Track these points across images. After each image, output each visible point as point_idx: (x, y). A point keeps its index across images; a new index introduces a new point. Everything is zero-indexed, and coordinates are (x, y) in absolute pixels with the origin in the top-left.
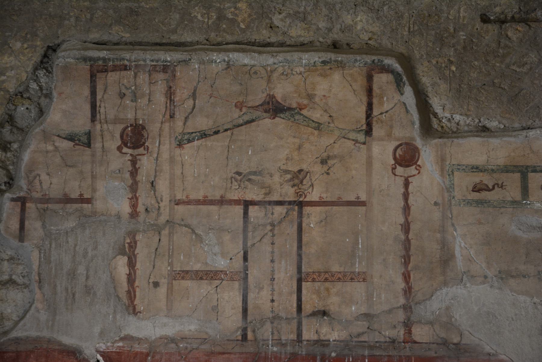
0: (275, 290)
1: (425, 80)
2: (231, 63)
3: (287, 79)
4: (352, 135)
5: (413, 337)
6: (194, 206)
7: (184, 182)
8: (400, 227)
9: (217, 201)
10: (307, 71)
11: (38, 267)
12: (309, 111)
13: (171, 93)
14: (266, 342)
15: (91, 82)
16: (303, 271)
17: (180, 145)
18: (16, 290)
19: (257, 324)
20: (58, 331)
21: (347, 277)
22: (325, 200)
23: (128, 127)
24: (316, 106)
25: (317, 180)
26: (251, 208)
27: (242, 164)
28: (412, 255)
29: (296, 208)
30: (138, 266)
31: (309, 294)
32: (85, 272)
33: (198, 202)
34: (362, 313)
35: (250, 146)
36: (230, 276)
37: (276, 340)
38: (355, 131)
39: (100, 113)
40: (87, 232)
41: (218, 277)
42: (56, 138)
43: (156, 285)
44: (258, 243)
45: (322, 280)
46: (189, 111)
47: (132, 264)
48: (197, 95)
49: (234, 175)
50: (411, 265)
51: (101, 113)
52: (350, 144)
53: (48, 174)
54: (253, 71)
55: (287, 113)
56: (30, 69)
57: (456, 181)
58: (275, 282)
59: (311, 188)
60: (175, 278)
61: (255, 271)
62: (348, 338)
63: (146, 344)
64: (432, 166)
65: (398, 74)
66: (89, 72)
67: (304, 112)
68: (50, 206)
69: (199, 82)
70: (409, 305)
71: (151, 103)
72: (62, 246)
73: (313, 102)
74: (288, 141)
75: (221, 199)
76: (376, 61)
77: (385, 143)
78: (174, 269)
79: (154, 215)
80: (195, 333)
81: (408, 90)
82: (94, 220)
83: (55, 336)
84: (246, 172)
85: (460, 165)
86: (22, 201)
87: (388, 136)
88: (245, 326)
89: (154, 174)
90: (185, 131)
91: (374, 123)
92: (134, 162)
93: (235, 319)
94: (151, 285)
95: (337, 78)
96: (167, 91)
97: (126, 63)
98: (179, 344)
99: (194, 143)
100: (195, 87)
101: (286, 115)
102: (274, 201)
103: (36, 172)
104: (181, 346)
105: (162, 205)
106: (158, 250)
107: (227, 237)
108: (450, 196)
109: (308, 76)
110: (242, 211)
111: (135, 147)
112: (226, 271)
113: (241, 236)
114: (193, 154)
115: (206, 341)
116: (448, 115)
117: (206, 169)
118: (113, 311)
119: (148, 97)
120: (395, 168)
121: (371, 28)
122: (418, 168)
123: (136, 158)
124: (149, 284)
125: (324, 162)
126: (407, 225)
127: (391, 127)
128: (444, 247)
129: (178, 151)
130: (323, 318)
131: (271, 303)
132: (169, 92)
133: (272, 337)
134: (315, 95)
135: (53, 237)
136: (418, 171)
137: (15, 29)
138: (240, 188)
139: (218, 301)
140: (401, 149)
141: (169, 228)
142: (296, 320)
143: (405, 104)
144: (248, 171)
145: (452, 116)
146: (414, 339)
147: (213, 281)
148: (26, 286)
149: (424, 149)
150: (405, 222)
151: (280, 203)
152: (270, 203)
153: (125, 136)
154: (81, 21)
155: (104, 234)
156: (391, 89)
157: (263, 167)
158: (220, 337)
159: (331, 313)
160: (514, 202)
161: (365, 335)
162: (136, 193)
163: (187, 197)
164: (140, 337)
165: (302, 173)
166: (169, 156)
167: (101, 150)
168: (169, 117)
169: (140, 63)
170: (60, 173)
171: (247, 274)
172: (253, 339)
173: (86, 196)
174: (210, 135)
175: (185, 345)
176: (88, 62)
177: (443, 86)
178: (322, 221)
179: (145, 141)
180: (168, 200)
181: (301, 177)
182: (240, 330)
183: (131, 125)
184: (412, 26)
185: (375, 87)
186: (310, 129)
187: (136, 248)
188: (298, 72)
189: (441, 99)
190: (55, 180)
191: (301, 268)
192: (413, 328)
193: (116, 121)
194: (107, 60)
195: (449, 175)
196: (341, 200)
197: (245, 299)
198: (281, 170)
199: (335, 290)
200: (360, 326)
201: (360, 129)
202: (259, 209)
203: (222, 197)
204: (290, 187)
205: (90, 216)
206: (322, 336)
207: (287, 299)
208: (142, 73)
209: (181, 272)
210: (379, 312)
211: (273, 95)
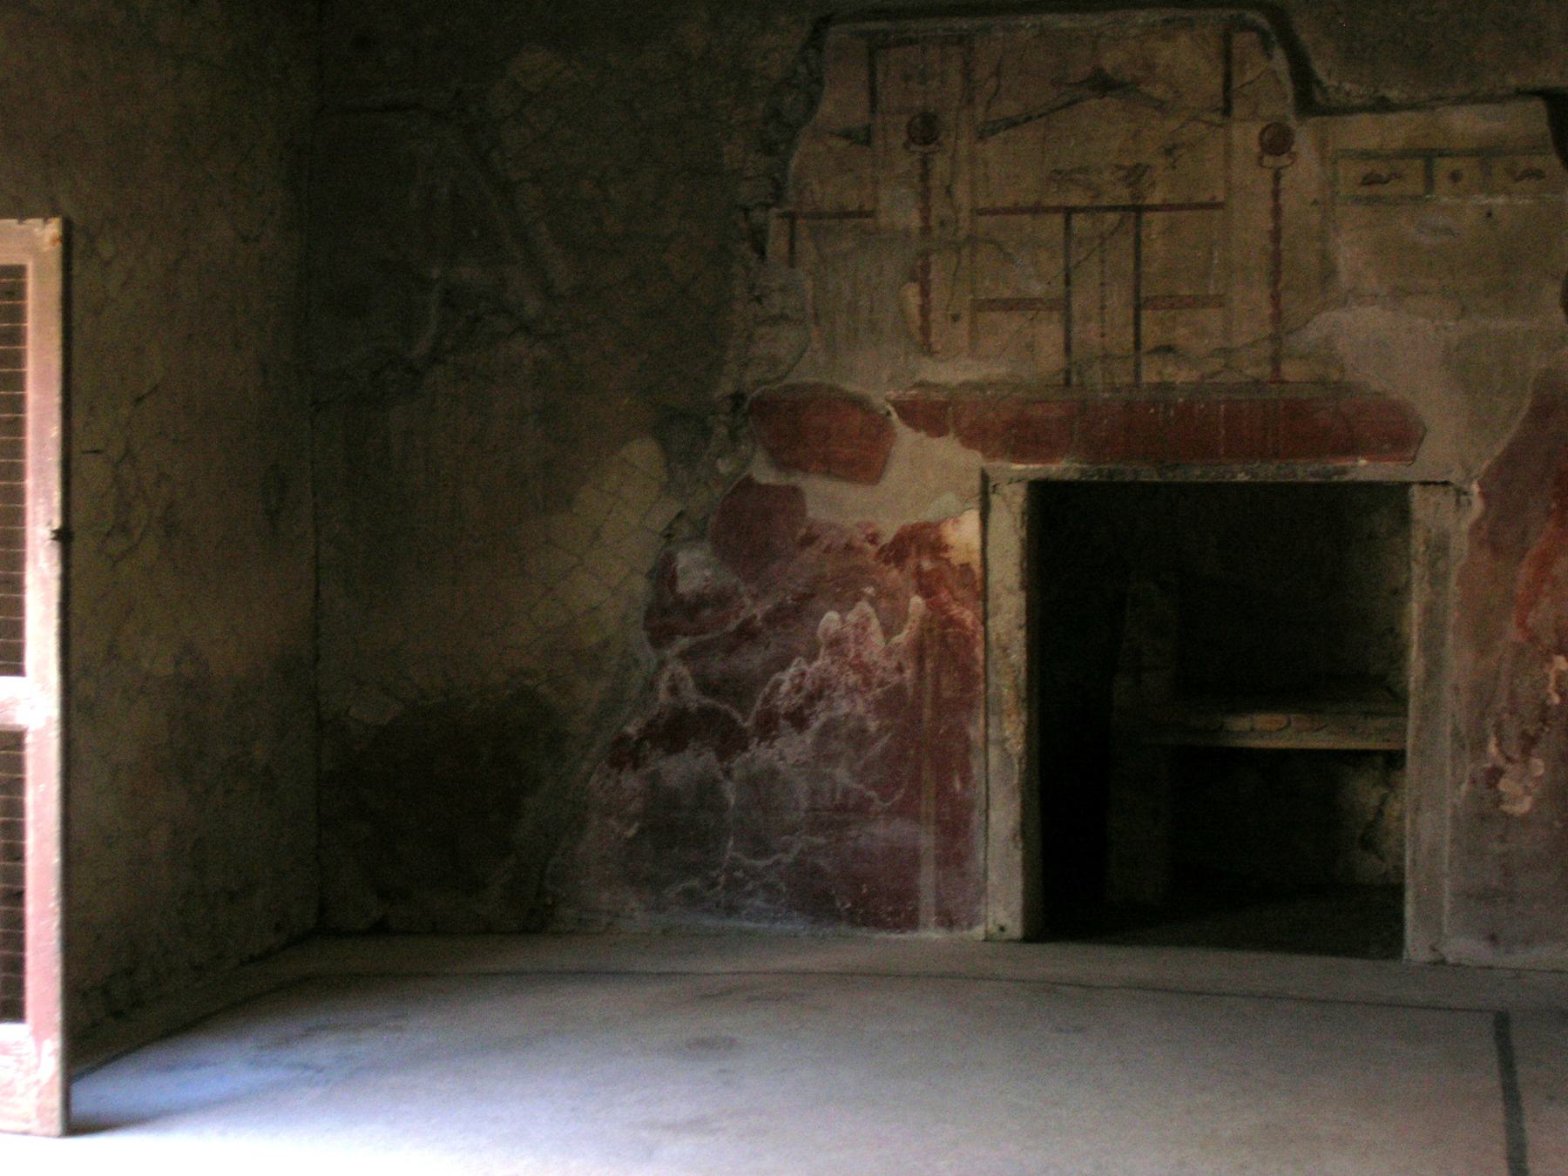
1: (1304, 38)
4: (1207, 117)
17: (982, 137)
30: (933, 295)
43: (956, 318)
47: (925, 293)
52: (1201, 126)
57: (1341, 172)
81: (1279, 54)
86: (792, 217)
92: (925, 162)
107: (1043, 256)
111: (926, 142)
116: (1336, 84)
125: (1169, 152)
129: (979, 146)
149: (1298, 130)
152: (1098, 209)
160: (1415, 198)
173: (867, 208)
200: (1217, 363)
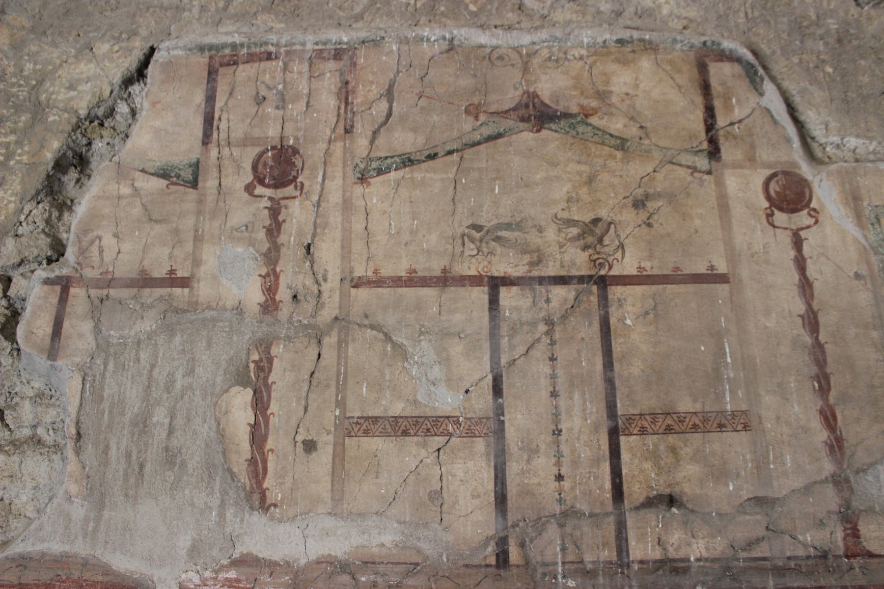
0: (565, 454)
2: (456, 42)
3: (558, 67)
4: (687, 159)
5: (865, 544)
6: (388, 289)
7: (370, 245)
8: (800, 321)
9: (435, 280)
10: (592, 55)
11: (77, 409)
12: (601, 119)
13: (347, 92)
14: (551, 568)
15: (208, 83)
16: (619, 413)
17: (363, 179)
18: (39, 457)
19: (530, 530)
20: (106, 542)
21: (710, 423)
22: (650, 273)
23: (268, 150)
24: (614, 110)
25: (630, 236)
26: (503, 292)
27: (482, 211)
28: (831, 373)
29: (595, 288)
30: (274, 408)
31: (637, 461)
32: (167, 421)
33: (397, 282)
34: (751, 496)
35: (495, 179)
36: (467, 427)
37: (573, 562)
38: (690, 152)
39: (218, 128)
40: (178, 339)
41: (441, 430)
42: (138, 174)
43: (310, 446)
44: (522, 359)
45: (661, 431)
46: (382, 119)
47: (260, 404)
48: (396, 95)
49: (466, 231)
51: (221, 131)
52: (682, 172)
53: (116, 236)
54: (495, 55)
55: (562, 122)
56: (117, 79)
58: (563, 438)
59: (620, 253)
60: (350, 433)
61: (519, 416)
63: (287, 574)
64: (839, 209)
65: (749, 63)
66: (207, 68)
67: (594, 120)
68: (112, 292)
69: (398, 72)
70: (843, 475)
71: (310, 109)
72: (126, 367)
73: (609, 105)
74: (569, 169)
75: (442, 275)
76: (709, 44)
77: (746, 172)
78: (348, 414)
79: (308, 306)
80: (394, 551)
82: (193, 317)
83: (98, 553)
84: (491, 224)
86: (64, 285)
87: (750, 160)
88: (502, 535)
89: (312, 232)
90: (372, 155)
91: (722, 140)
92: (275, 211)
93: (480, 518)
94: (300, 446)
95: (647, 65)
96: (340, 89)
97: (272, 49)
98: (358, 576)
99: (388, 175)
100: (391, 80)
101: (562, 126)
102: (549, 277)
103: (95, 233)
104: (363, 579)
105: (325, 287)
106: (316, 375)
107: (457, 349)
109: (595, 62)
110: (486, 298)
111: (278, 184)
112: (458, 417)
113: (486, 345)
115: (419, 568)
116: (836, 139)
117: (413, 220)
118: (218, 502)
119: (306, 100)
120: (772, 215)
121: (684, 14)
122: (812, 213)
123: (279, 204)
124: (295, 446)
125: (639, 204)
126: (812, 316)
127: (753, 146)
129: (359, 190)
130: (669, 510)
131: (557, 483)
132: (344, 90)
133: (564, 556)
134: (611, 92)
136: (813, 220)
137: (105, 27)
138: (480, 253)
139: (441, 479)
140: (777, 182)
141: (340, 332)
142: (612, 518)
143: (768, 110)
144: (495, 222)
145: (842, 139)
146: (867, 548)
147: (431, 438)
148: (57, 448)
150: (807, 310)
151: (562, 280)
152: (541, 280)
153: (260, 167)
154: (209, 11)
155: (209, 345)
156: (742, 87)
158: (448, 560)
159: (685, 499)
161: (762, 544)
162: (275, 265)
163: (376, 272)
164: (276, 558)
165: (600, 224)
166: (341, 199)
168: (342, 132)
169: (294, 48)
170: (137, 234)
171: (503, 422)
172: (521, 562)
173: (179, 274)
174: (419, 162)
175: (372, 577)
176: (207, 52)
177: (818, 95)
178: (647, 313)
179: (298, 173)
180: (338, 278)
181: (598, 231)
182: (493, 543)
183: (273, 148)
184: (749, 11)
185: (714, 82)
186: (607, 148)
188: (577, 55)
189: (819, 114)
190: (126, 247)
191: (615, 406)
192: (860, 523)
193: (246, 141)
194: (239, 47)
195: (872, 224)
196: (679, 273)
198: (560, 220)
199: (688, 450)
201: (698, 149)
202: (520, 292)
203: (444, 271)
204: (579, 251)
206: (671, 549)
207: (590, 472)
208: (297, 62)
209: (362, 421)
210: (784, 493)
211: (534, 92)
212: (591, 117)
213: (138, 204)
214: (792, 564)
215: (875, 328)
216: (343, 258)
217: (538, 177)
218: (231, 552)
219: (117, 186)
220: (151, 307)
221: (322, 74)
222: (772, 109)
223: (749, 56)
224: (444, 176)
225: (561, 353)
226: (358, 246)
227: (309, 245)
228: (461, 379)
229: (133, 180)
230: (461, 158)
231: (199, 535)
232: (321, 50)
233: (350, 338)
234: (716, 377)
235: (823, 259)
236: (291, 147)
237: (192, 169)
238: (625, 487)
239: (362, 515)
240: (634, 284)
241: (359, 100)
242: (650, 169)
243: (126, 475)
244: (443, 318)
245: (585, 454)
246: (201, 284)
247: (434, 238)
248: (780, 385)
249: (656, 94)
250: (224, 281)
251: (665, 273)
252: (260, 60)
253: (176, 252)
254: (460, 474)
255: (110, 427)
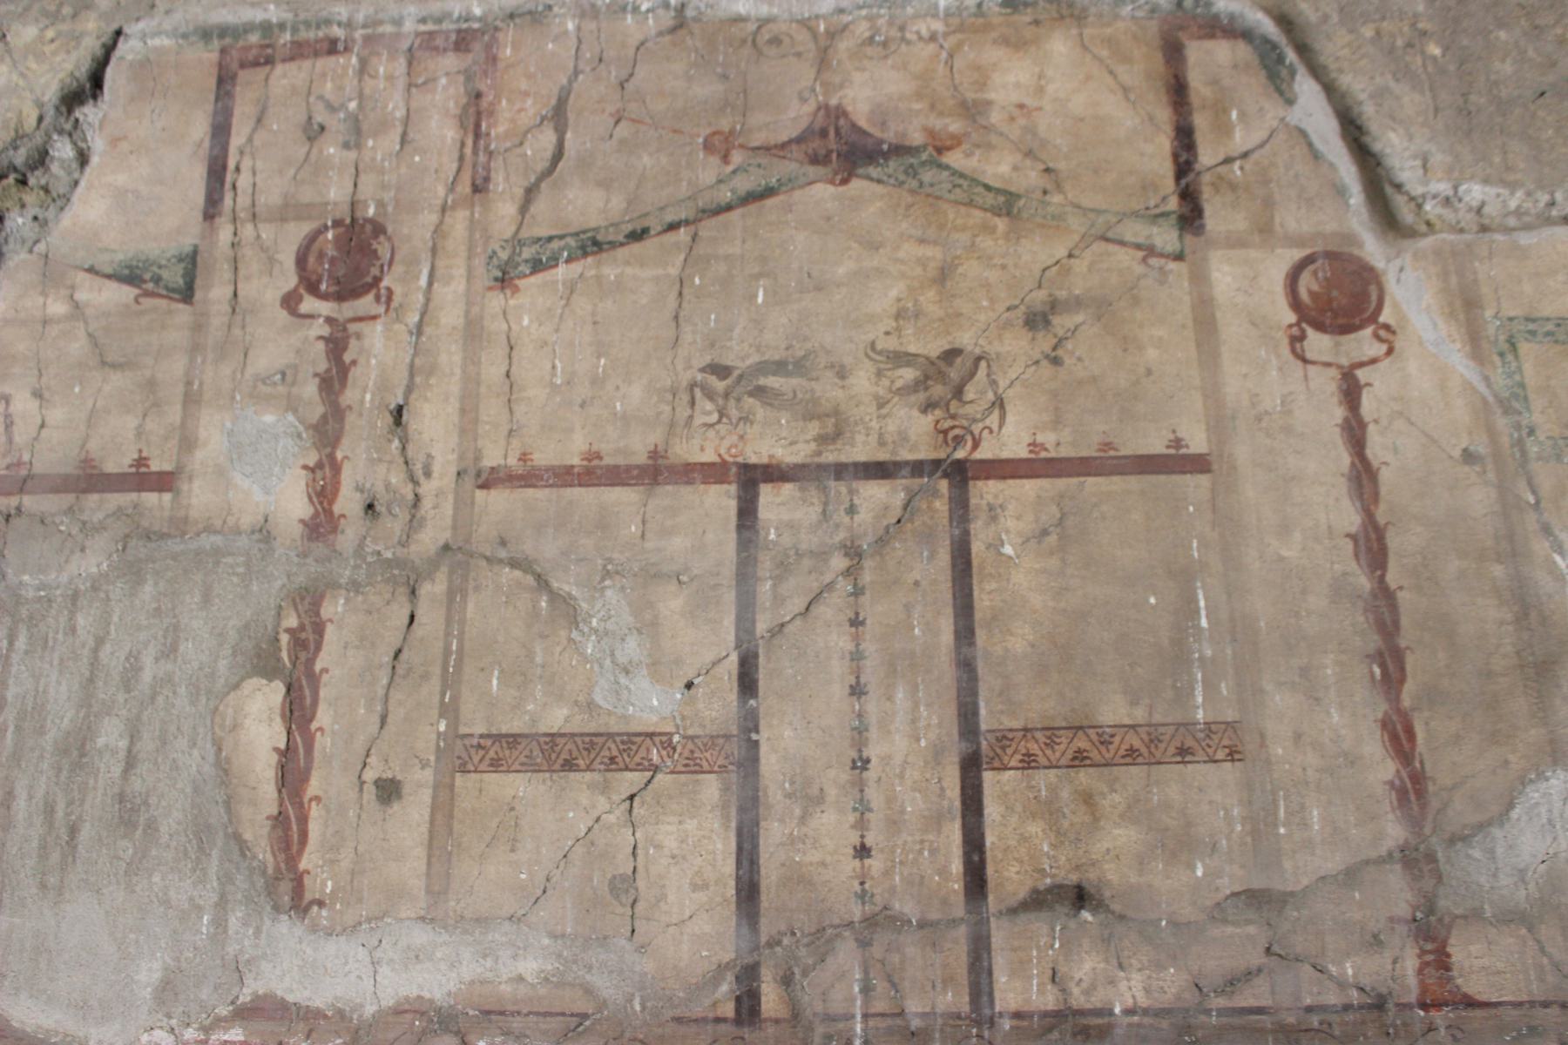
0: (874, 805)
2: (690, 13)
3: (886, 57)
4: (1135, 231)
5: (1459, 981)
6: (547, 491)
7: (515, 407)
8: (1349, 546)
9: (635, 472)
10: (954, 32)
12: (968, 155)
13: (479, 114)
14: (841, 1025)
15: (217, 99)
16: (983, 727)
17: (504, 280)
19: (803, 952)
21: (1162, 746)
22: (1053, 454)
23: (326, 228)
24: (994, 139)
25: (1017, 383)
26: (766, 493)
27: (730, 339)
28: (1408, 648)
29: (944, 485)
30: (323, 717)
31: (1014, 820)
32: (123, 744)
33: (565, 476)
34: (1237, 888)
36: (687, 753)
37: (883, 1015)
38: (1143, 216)
39: (234, 187)
40: (148, 589)
41: (637, 759)
43: (389, 790)
44: (798, 622)
45: (1063, 762)
46: (541, 166)
47: (298, 712)
48: (571, 116)
49: (699, 377)
50: (1409, 689)
51: (239, 191)
52: (1126, 259)
53: (38, 394)
54: (765, 35)
55: (892, 164)
56: (51, 94)
58: (871, 775)
59: (996, 413)
60: (464, 764)
61: (788, 733)
62: (1187, 995)
64: (1435, 325)
65: (1266, 40)
66: (215, 71)
68: (27, 501)
69: (576, 72)
70: (1422, 848)
71: (408, 148)
72: (51, 643)
73: (985, 128)
74: (901, 254)
75: (650, 462)
77: (1253, 254)
78: (463, 730)
79: (394, 525)
80: (542, 991)
81: (1306, 88)
84: (749, 362)
85: (1533, 320)
87: (1261, 231)
88: (749, 960)
89: (405, 382)
90: (524, 234)
91: (1206, 194)
92: (336, 344)
93: (707, 928)
94: (370, 790)
96: (465, 108)
97: (338, 32)
99: (553, 271)
100: (562, 88)
101: (890, 170)
102: (856, 465)
105: (427, 488)
106: (404, 656)
107: (672, 603)
108: (1518, 427)
109: (960, 45)
110: (732, 505)
112: (671, 735)
113: (730, 597)
114: (549, 310)
115: (587, 1023)
116: (1443, 187)
117: (598, 358)
118: (215, 898)
119: (399, 130)
120: (1302, 337)
122: (1382, 333)
123: (345, 329)
124: (361, 790)
125: (1036, 321)
126: (1373, 536)
127: (1269, 203)
128: (1526, 615)
129: (496, 301)
131: (857, 863)
132: (472, 110)
133: (866, 1003)
134: (989, 103)
135: (24, 612)
136: (1384, 348)
138: (724, 420)
139: (634, 854)
140: (1315, 273)
141: (451, 573)
142: (962, 931)
143: (1303, 133)
144: (755, 359)
145: (1456, 188)
146: (1465, 989)
147: (618, 775)
150: (1364, 525)
151: (880, 470)
152: (840, 471)
153: (311, 260)
155: (207, 599)
156: (1251, 88)
157: (809, 345)
158: (644, 1008)
159: (1107, 894)
161: (1258, 981)
163: (524, 458)
164: (318, 1003)
165: (959, 360)
166: (462, 320)
167: (227, 308)
168: (468, 190)
169: (380, 30)
170: (77, 390)
171: (756, 743)
172: (782, 1012)
173: (155, 466)
174: (613, 245)
177: (1411, 101)
178: (1045, 532)
179: (382, 271)
180: (453, 470)
181: (954, 374)
182: (730, 977)
183: (337, 223)
186: (977, 213)
187: (318, 648)
189: (1411, 138)
190: (56, 415)
191: (976, 713)
192: (1452, 941)
193: (287, 212)
194: (276, 30)
195: (1501, 355)
196: (1112, 453)
197: (747, 846)
198: (880, 353)
199: (1117, 798)
201: (1158, 211)
202: (798, 494)
203: (654, 454)
204: (915, 413)
205: (163, 536)
206: (1076, 991)
207: (922, 842)
208: (384, 57)
209: (489, 742)
210: (1305, 881)
212: (949, 154)
213: (81, 333)
214: (1315, 1021)
215: (1499, 561)
216: (463, 432)
217: (841, 271)
218: (235, 992)
219: (41, 300)
220: (101, 528)
221: (432, 80)
222: (1310, 131)
223: (1269, 27)
224: (660, 272)
225: (876, 611)
226: (492, 410)
227: (399, 410)
228: (678, 662)
229: (73, 287)
230: (694, 238)
231: (178, 960)
232: (431, 34)
233: (471, 584)
234: (1178, 657)
235: (1399, 424)
236: (367, 220)
237: (182, 265)
238: (990, 870)
239: (482, 921)
240: (1021, 477)
241: (501, 129)
242: (1061, 252)
243: (44, 849)
244: (649, 545)
245: (914, 805)
246: (196, 484)
247: (636, 392)
248: (1304, 671)
249: (1078, 104)
250: (238, 478)
251: (1084, 453)
252: (316, 54)
253: (150, 425)
254: (671, 844)
255: (17, 757)
